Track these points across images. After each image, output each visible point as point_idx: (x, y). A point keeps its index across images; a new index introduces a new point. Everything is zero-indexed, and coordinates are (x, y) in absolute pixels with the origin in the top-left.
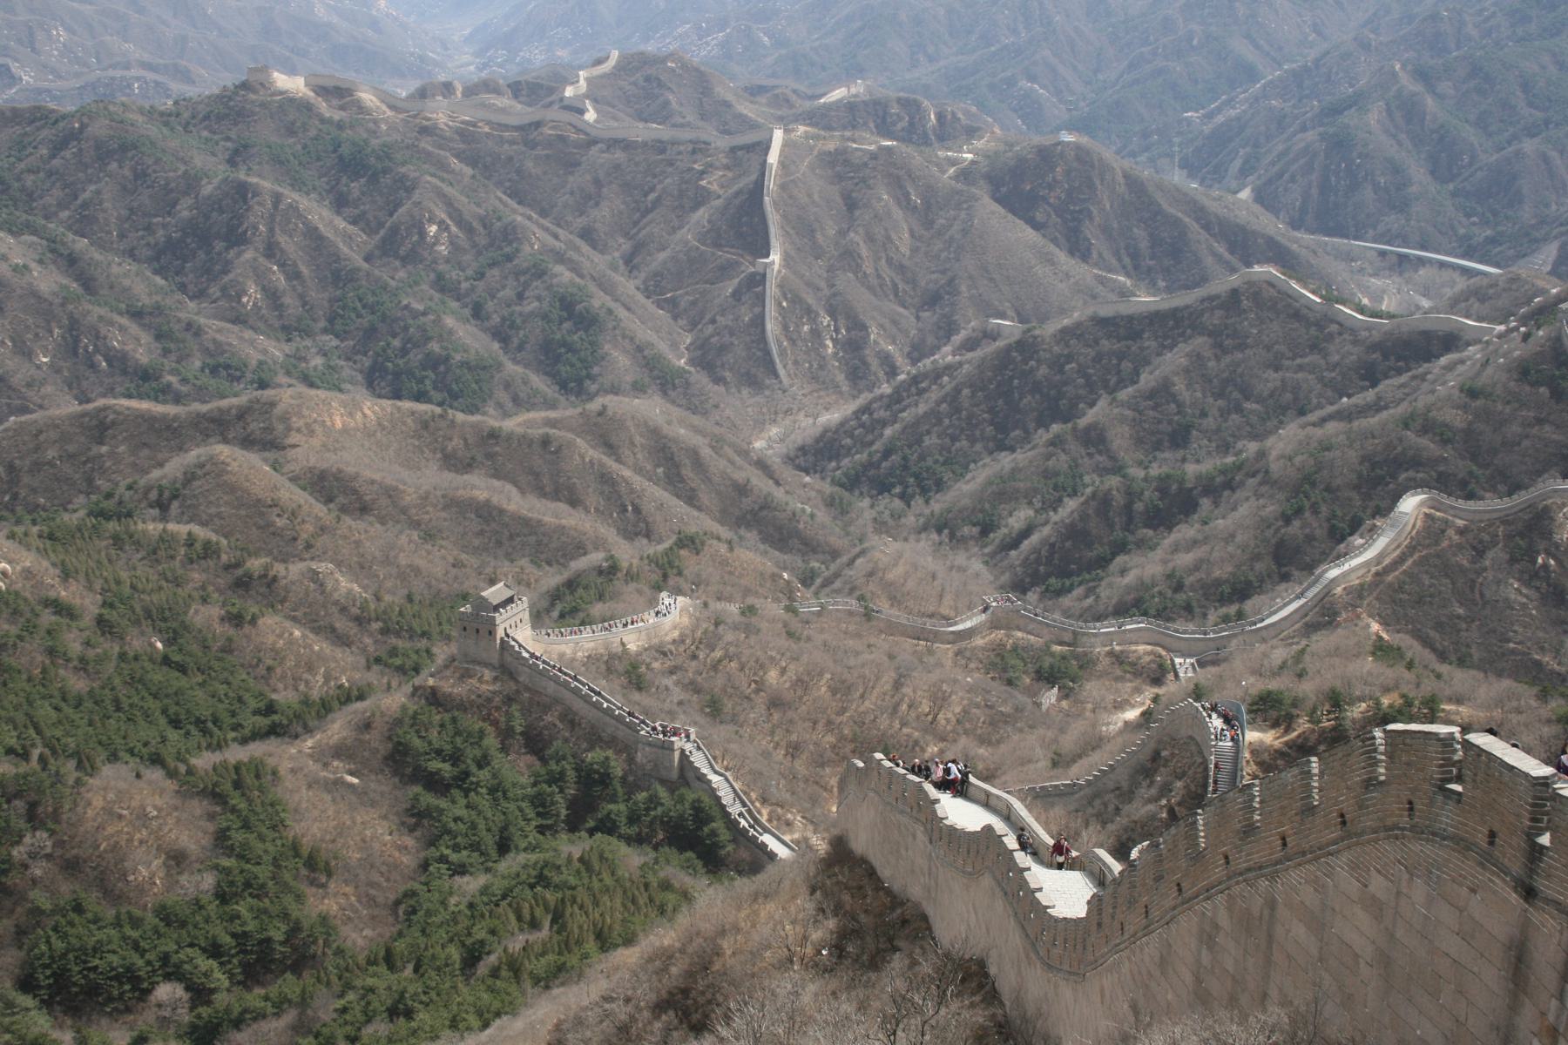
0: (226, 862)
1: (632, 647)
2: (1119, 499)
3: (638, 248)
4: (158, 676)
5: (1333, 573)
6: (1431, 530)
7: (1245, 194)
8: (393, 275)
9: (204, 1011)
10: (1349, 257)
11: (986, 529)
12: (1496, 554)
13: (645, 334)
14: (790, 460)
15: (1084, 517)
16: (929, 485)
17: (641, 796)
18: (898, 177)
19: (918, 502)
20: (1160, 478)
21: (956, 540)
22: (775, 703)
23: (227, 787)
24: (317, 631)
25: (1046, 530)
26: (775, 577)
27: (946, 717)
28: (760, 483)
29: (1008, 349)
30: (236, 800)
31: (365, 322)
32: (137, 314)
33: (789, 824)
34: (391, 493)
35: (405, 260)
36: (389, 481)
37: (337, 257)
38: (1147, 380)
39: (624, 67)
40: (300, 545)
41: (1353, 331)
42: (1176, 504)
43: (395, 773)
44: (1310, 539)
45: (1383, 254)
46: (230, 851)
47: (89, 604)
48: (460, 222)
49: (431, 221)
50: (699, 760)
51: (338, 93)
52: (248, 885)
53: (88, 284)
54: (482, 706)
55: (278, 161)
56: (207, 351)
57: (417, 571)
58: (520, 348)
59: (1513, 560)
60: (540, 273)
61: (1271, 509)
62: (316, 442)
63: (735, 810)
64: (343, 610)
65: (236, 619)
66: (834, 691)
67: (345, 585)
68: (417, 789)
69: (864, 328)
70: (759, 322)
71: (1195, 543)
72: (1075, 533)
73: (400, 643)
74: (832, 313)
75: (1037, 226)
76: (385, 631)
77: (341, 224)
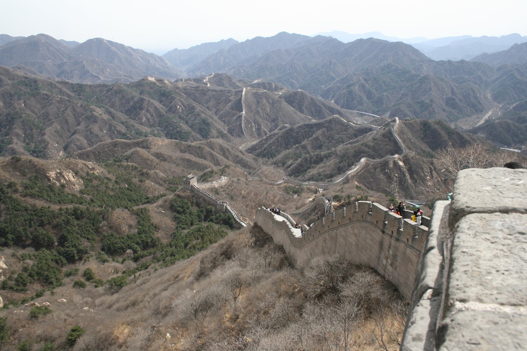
0: (140, 227)
1: (216, 186)
2: (309, 159)
3: (217, 110)
4: (126, 192)
5: (349, 172)
6: (367, 165)
7: (333, 101)
8: (171, 115)
9: (136, 255)
10: (352, 114)
11: (284, 164)
12: (378, 170)
13: (219, 127)
14: (246, 151)
15: (302, 162)
16: (273, 156)
17: (218, 215)
18: (267, 98)
19: (271, 159)
20: (317, 155)
21: (278, 166)
22: (244, 197)
23: (139, 213)
24: (156, 183)
25: (295, 164)
26: (243, 173)
27: (276, 200)
28: (241, 155)
29: (288, 130)
30: (141, 215)
31: (165, 124)
32: (122, 123)
33: (246, 220)
34: (170, 157)
35: (173, 113)
36: (170, 155)
37: (160, 112)
38: (314, 136)
39: (215, 76)
40: (153, 167)
41: (353, 127)
42: (319, 160)
43: (171, 210)
44: (344, 166)
45: (358, 113)
46: (140, 225)
47: (114, 178)
48: (184, 105)
50: (229, 208)
51: (161, 81)
52: (144, 231)
53: (113, 117)
54: (188, 198)
55: (149, 94)
56: (135, 130)
57: (175, 172)
58: (195, 129)
59: (381, 171)
60: (199, 115)
61: (337, 161)
62: (156, 147)
63: (235, 216)
64: (161, 179)
65: (141, 181)
66: (255, 195)
67: (162, 174)
68: (175, 213)
69: (260, 126)
70: (241, 124)
71: (323, 167)
72: (300, 165)
73: (172, 186)
74: (255, 123)
75: (293, 107)
76: (169, 183)
77: (161, 106)
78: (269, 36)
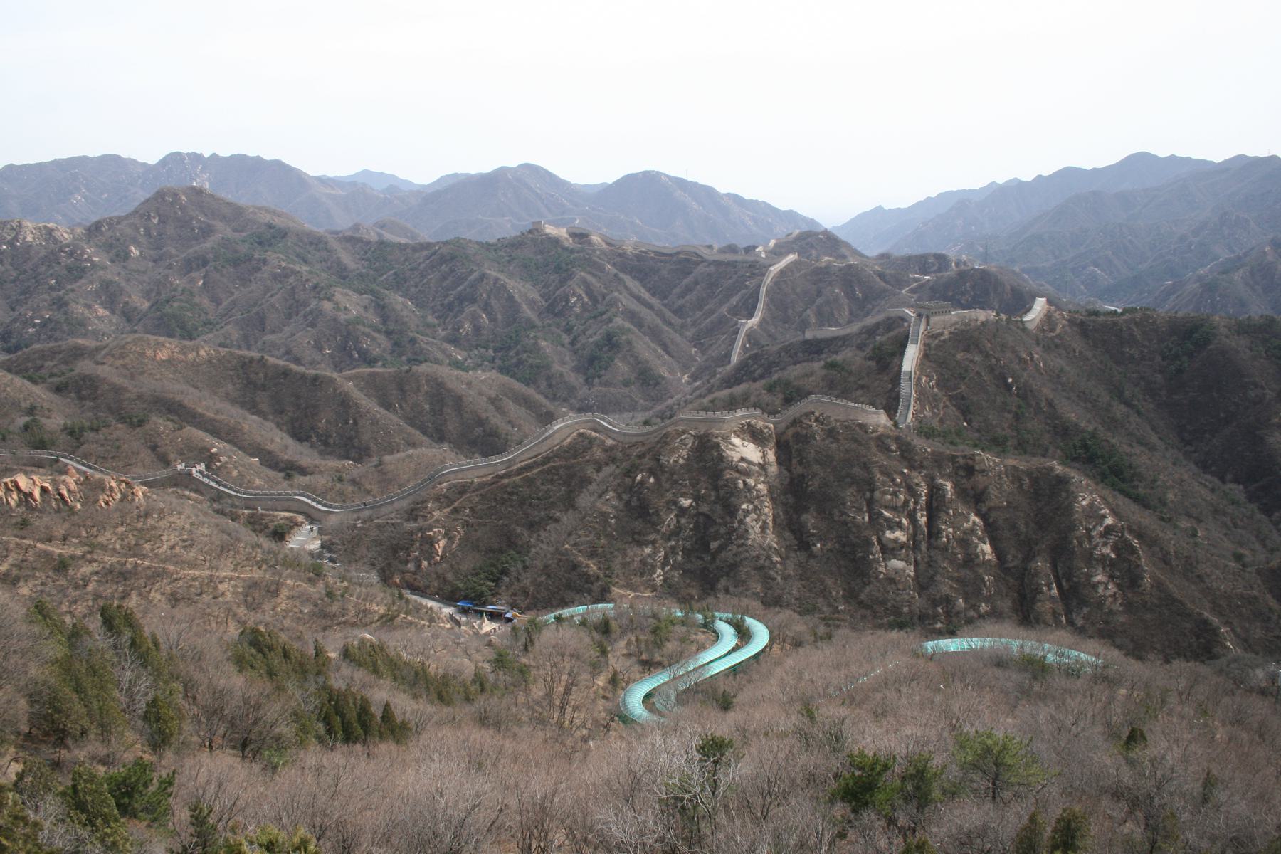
49: (574, 295)
78: (1100, 165)
